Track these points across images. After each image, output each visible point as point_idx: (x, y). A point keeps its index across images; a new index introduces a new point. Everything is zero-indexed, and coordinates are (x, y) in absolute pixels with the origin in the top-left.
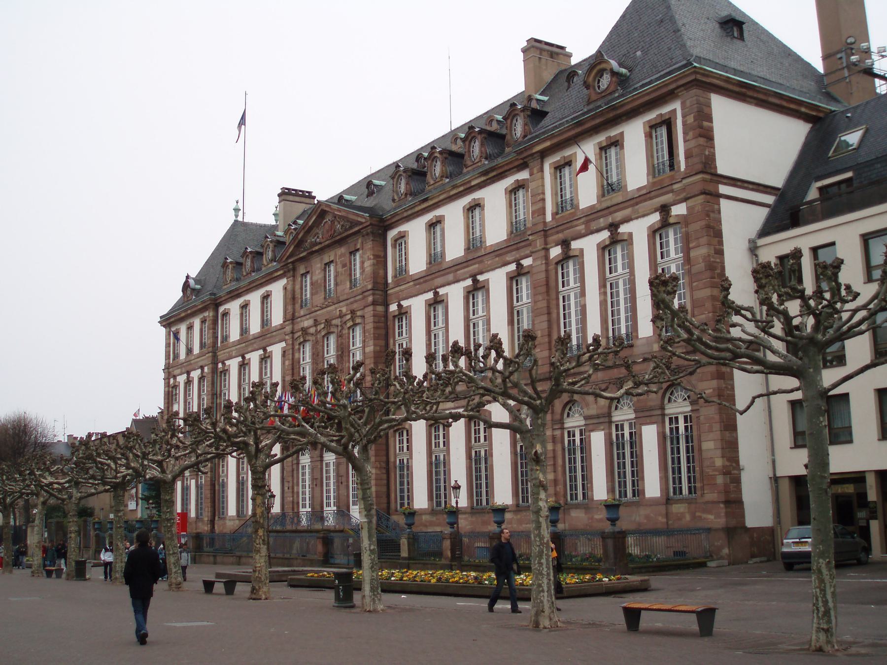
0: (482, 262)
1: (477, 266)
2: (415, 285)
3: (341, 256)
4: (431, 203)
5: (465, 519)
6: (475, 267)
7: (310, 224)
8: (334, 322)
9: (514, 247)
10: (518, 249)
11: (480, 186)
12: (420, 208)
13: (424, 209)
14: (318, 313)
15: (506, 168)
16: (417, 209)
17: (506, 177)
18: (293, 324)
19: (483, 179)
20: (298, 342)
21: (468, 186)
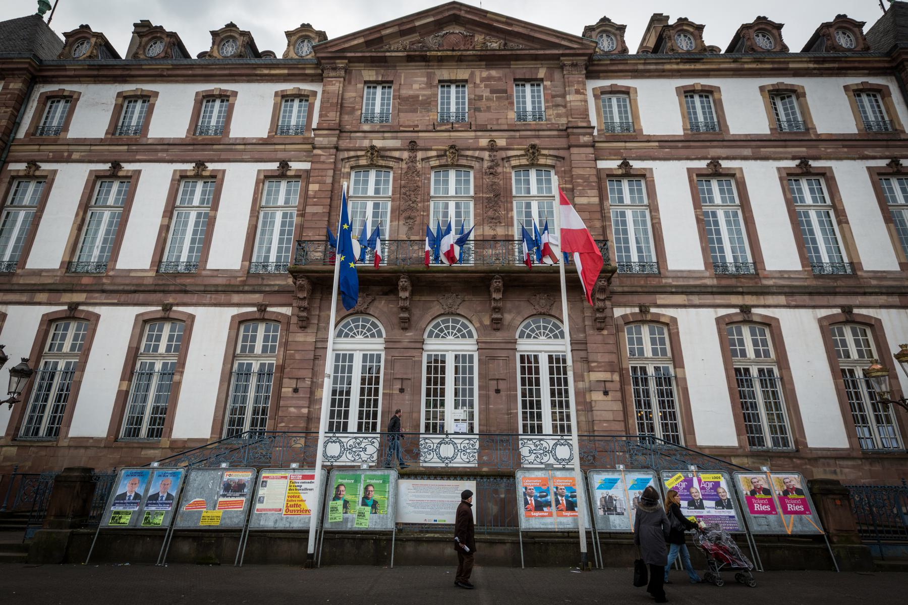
0: (816, 147)
1: (804, 149)
2: (661, 147)
3: (483, 80)
4: (699, 66)
5: (853, 467)
6: (802, 151)
7: (417, 24)
8: (469, 153)
9: (884, 143)
10: (887, 147)
11: (797, 73)
12: (675, 67)
13: (679, 71)
14: (420, 134)
15: (856, 65)
16: (668, 67)
17: (845, 75)
18: (339, 137)
19: (811, 66)
20: (353, 163)
21: (782, 66)
